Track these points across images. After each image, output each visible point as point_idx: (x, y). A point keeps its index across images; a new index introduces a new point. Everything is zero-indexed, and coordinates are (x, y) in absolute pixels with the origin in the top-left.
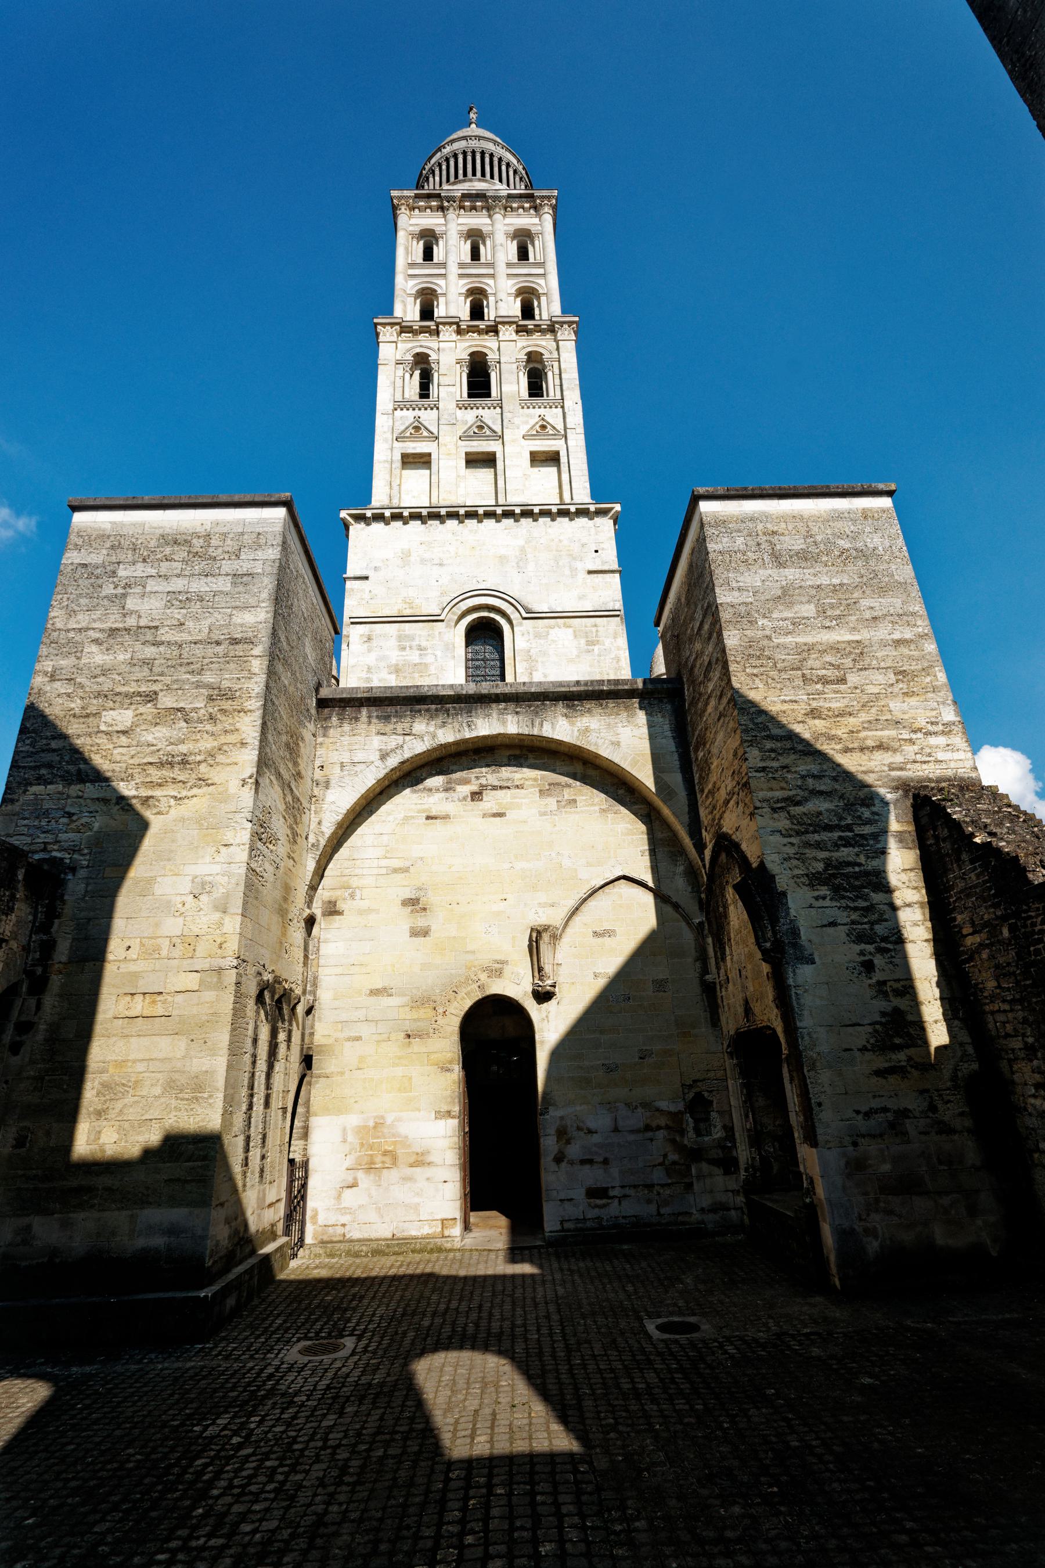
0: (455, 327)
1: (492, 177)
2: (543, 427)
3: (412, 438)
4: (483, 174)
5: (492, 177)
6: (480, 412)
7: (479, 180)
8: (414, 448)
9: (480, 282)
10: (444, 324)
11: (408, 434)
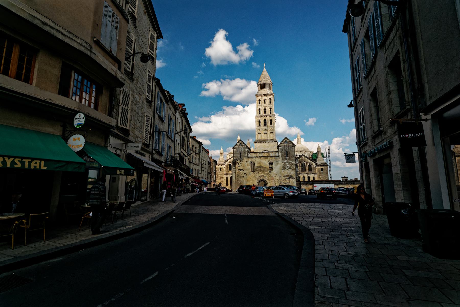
3: (259, 131)
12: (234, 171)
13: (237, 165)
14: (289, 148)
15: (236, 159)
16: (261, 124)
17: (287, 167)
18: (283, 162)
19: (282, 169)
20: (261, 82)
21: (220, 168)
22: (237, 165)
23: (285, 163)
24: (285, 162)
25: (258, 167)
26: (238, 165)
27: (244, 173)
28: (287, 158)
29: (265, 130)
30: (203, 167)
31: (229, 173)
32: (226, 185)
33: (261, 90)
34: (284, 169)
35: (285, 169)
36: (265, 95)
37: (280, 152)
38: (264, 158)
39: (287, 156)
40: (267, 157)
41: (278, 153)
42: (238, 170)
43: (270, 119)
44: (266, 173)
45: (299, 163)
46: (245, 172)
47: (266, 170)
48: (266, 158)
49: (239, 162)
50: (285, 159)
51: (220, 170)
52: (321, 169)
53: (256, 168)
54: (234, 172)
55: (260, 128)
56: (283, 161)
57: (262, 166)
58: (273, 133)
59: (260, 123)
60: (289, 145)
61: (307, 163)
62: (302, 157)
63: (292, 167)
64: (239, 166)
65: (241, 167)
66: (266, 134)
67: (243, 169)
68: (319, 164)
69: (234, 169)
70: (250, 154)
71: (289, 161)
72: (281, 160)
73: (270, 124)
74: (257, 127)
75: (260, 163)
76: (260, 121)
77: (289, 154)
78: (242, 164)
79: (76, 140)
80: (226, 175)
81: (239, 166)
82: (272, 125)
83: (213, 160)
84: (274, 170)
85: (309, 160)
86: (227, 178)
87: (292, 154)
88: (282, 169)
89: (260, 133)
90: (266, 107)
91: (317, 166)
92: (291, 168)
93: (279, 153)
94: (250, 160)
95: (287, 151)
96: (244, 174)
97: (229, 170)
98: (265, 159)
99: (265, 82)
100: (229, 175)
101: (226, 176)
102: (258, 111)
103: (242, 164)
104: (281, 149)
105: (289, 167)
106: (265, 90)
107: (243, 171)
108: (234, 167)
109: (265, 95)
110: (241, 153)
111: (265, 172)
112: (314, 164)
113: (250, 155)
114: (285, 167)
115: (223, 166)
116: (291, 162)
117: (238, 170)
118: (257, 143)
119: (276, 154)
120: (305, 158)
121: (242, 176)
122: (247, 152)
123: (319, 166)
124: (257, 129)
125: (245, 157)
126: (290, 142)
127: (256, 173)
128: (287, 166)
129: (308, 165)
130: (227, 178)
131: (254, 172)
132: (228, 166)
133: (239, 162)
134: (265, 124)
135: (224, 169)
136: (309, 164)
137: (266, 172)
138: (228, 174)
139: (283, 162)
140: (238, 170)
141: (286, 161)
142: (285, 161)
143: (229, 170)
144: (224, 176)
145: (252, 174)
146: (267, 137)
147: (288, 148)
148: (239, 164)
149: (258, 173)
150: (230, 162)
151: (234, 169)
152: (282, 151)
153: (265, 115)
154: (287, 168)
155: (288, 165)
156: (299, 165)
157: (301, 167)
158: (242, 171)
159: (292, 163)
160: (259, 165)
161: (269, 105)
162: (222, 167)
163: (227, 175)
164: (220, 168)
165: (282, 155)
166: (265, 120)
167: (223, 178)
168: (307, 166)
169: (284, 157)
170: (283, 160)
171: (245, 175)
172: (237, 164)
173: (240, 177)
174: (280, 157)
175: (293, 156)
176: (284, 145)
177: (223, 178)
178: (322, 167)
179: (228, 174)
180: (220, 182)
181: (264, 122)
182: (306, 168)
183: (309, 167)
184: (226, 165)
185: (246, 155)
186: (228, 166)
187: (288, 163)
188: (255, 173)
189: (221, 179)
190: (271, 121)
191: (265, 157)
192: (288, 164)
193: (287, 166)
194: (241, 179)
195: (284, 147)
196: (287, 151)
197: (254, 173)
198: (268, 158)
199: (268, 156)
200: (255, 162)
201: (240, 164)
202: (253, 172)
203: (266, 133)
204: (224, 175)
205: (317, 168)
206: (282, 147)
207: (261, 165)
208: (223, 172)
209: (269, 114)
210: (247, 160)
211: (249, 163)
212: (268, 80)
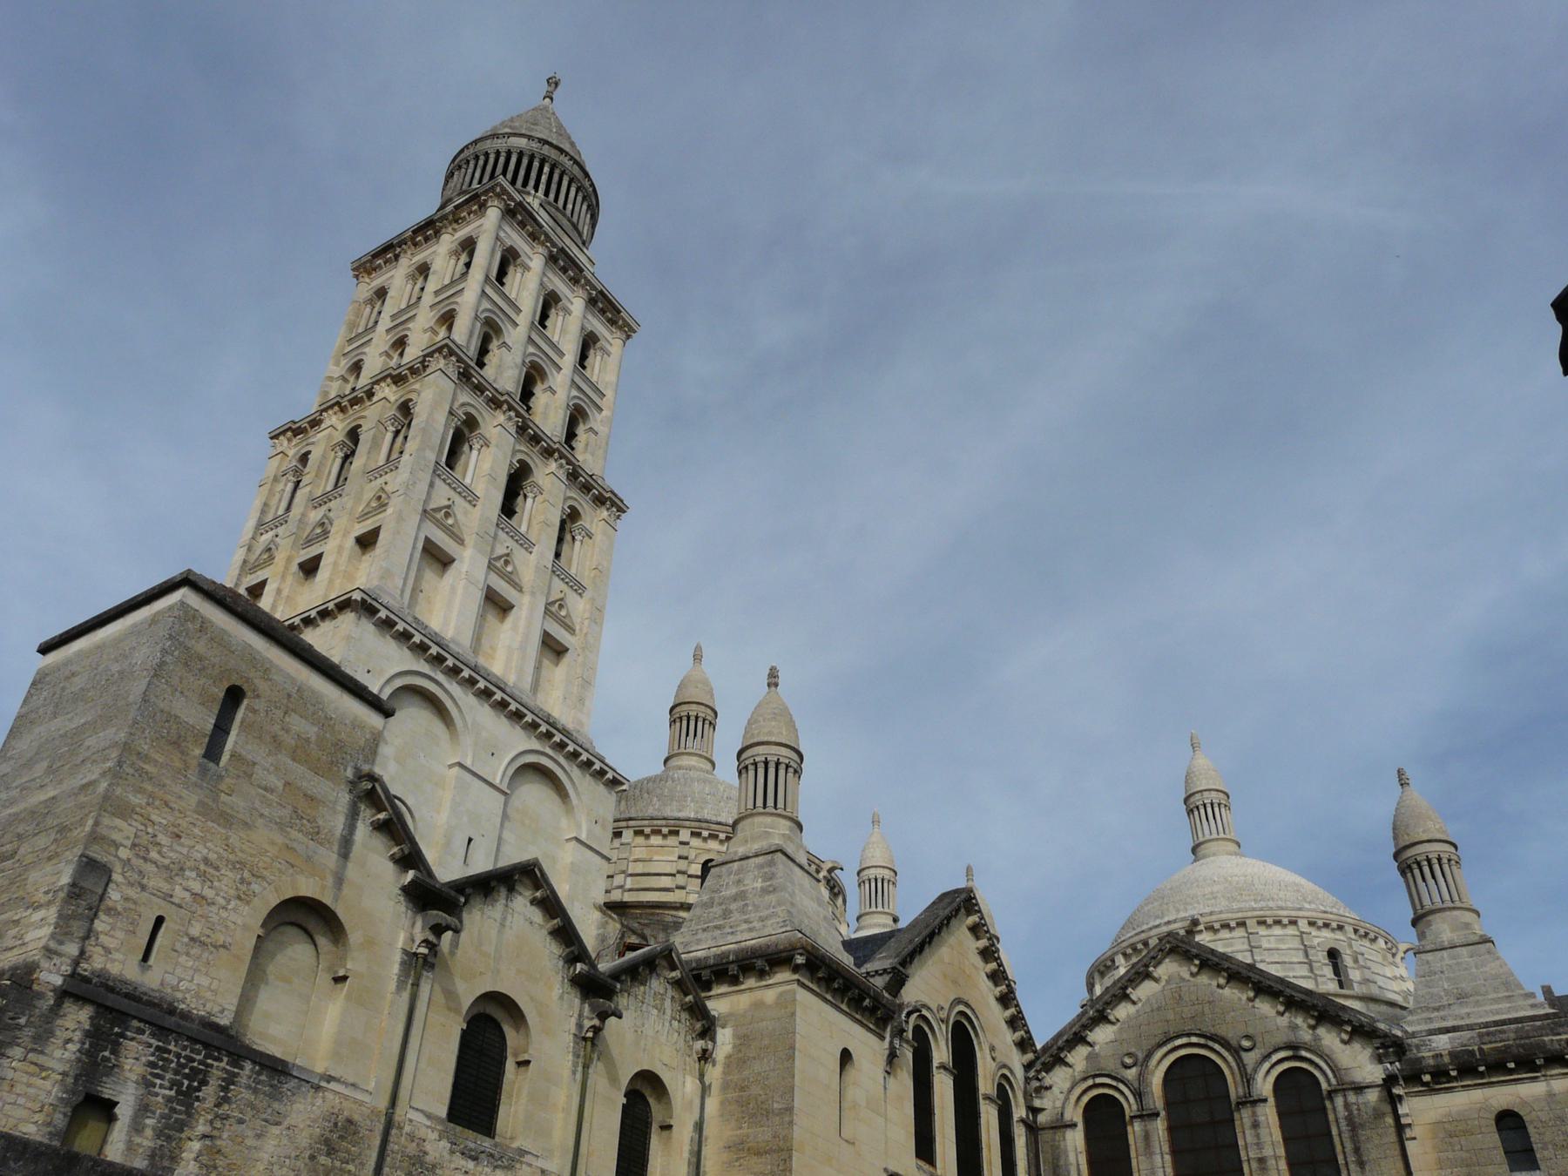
0: (336, 408)
45: (1131, 1074)
52: (1492, 1139)
61: (1249, 1058)
68: (1443, 1043)
91: (1413, 1077)
112: (1363, 1065)
123: (1439, 1077)
129: (1264, 1085)
156: (1130, 1106)
157: (1160, 1125)
168: (1251, 1101)
178: (1503, 1095)
182: (1245, 1137)
205: (1421, 1110)
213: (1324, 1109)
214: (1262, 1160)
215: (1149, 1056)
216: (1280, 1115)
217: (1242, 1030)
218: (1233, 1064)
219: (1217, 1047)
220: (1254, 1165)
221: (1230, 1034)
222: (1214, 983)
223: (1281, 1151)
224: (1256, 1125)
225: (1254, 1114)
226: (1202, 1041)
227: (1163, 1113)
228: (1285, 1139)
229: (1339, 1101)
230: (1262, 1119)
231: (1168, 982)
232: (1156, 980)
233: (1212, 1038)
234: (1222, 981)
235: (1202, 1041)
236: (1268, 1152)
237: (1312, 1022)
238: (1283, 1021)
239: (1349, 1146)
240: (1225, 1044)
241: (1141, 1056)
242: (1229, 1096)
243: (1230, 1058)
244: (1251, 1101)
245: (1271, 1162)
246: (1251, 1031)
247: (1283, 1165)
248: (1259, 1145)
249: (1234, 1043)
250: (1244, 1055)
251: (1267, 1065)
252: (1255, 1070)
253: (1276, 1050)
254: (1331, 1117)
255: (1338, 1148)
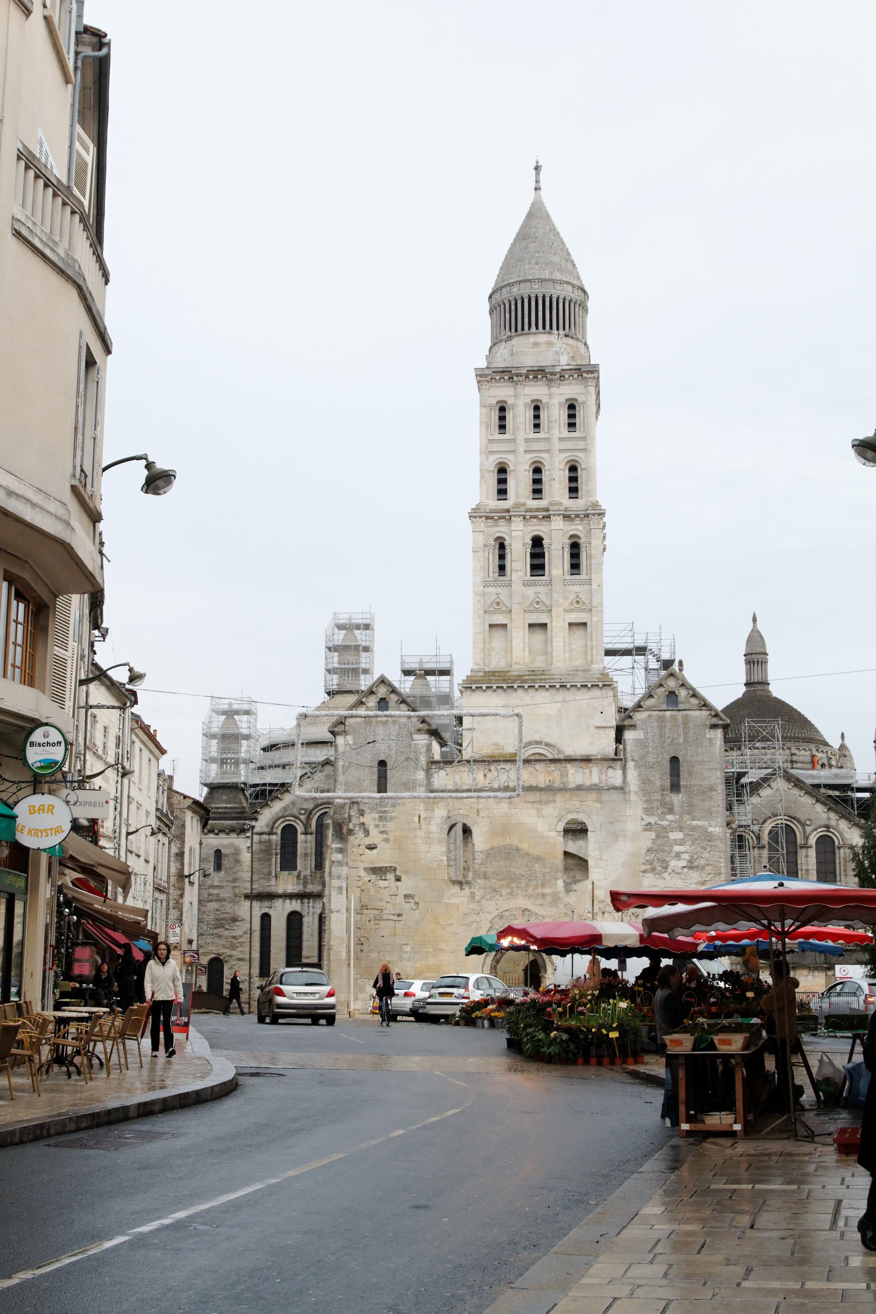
1: (551, 328)
2: (578, 602)
3: (495, 612)
4: (544, 328)
5: (551, 328)
6: (538, 589)
7: (541, 333)
8: (497, 620)
9: (539, 457)
10: (515, 516)
11: (492, 609)
12: (339, 877)
13: (357, 842)
14: (691, 734)
15: (354, 803)
16: (508, 568)
17: (678, 856)
18: (648, 827)
19: (644, 872)
20: (515, 290)
21: (218, 854)
22: (358, 839)
23: (661, 833)
24: (664, 828)
25: (491, 854)
26: (368, 841)
27: (402, 893)
28: (677, 799)
29: (537, 605)
30: (131, 852)
31: (280, 891)
32: (256, 970)
33: (515, 341)
34: (653, 870)
35: (666, 868)
36: (539, 374)
37: (630, 765)
38: (533, 796)
39: (675, 787)
40: (549, 789)
41: (618, 764)
42: (364, 868)
43: (572, 536)
44: (544, 895)
46: (407, 885)
47: (544, 874)
48: (545, 796)
49: (369, 819)
50: (663, 804)
51: (218, 867)
53: (480, 857)
54: (340, 888)
55: (503, 592)
56: (652, 820)
57: (520, 846)
58: (585, 624)
59: (502, 557)
60: (687, 716)
62: (773, 785)
63: (706, 855)
64: (371, 848)
65: (383, 857)
66: (539, 635)
67: (395, 870)
69: (340, 863)
70: (442, 773)
71: (686, 817)
72: (639, 812)
73: (567, 566)
74: (486, 584)
75: (503, 829)
76: (502, 547)
77: (690, 774)
78: (390, 835)
79: (39, 813)
80: (256, 904)
81: (371, 848)
82: (583, 576)
83: (188, 802)
84: (595, 873)
85: (819, 808)
86: (266, 919)
87: (706, 774)
88: (644, 872)
89: (504, 626)
90: (545, 456)
92: (702, 862)
93: (624, 769)
94: (440, 812)
95: (674, 760)
96: (400, 899)
97: (281, 870)
98: (540, 802)
99: (537, 290)
100: (278, 903)
101: (259, 908)
102: (493, 478)
103: (390, 835)
104: (638, 741)
105: (686, 856)
106: (543, 338)
107: (398, 879)
108: (340, 851)
109: (539, 374)
110: (382, 764)
111: (536, 887)
113: (442, 778)
114: (660, 855)
115: (242, 843)
116: (699, 823)
117: (364, 868)
118: (479, 693)
119: (610, 771)
120: (796, 792)
121: (389, 910)
122: (423, 759)
124: (484, 594)
125: (408, 786)
126: (694, 701)
127: (478, 894)
128: (677, 848)
129: (812, 841)
130: (266, 919)
131: (468, 883)
132: (274, 837)
133: (369, 819)
134: (538, 566)
135: (246, 857)
136: (821, 832)
137: (543, 885)
138: (271, 896)
139: (648, 827)
140: (362, 873)
141: (670, 817)
142: (662, 817)
143: (283, 868)
144: (244, 908)
145: (454, 901)
146: (547, 652)
147: (682, 740)
148: (373, 831)
149: (495, 891)
150: (285, 809)
151: (340, 863)
152: (642, 757)
153: (538, 510)
154: (674, 864)
155: (681, 843)
157: (765, 853)
158: (391, 876)
159: (705, 830)
160: (499, 842)
161: (561, 439)
162: (231, 845)
163: (267, 903)
164: (218, 854)
165: (645, 782)
166: (537, 542)
167: (235, 920)
168: (806, 846)
169: (657, 796)
170: (648, 811)
171: (407, 906)
172: (361, 834)
173: (378, 919)
174: (633, 797)
175: (712, 789)
176: (662, 720)
177: (235, 920)
179: (271, 896)
180: (212, 948)
181: (533, 556)
183: (817, 852)
184: (261, 834)
185: (421, 775)
186: (276, 838)
187: (681, 829)
188: (472, 895)
189: (226, 933)
190: (575, 548)
191: (541, 790)
192: (679, 835)
193: (677, 848)
194: (385, 928)
195: (661, 728)
196: (674, 760)
197: (467, 891)
198: (559, 797)
199: (557, 784)
200: (476, 823)
201: (375, 837)
202: (457, 889)
203: (544, 626)
204: (247, 903)
206: (646, 732)
207: (515, 842)
208: (235, 880)
209: (567, 502)
210: (421, 807)
211: (434, 828)
212: (558, 276)
213: (834, 853)
214: (807, 870)
215: (764, 823)
216: (817, 853)
217: (807, 816)
218: (801, 830)
219: (795, 822)
220: (804, 872)
221: (802, 818)
222: (798, 794)
223: (815, 867)
224: (807, 856)
225: (807, 852)
226: (789, 819)
227: (767, 846)
228: (817, 862)
229: (842, 851)
230: (809, 854)
231: (777, 790)
232: (772, 788)
233: (793, 818)
234: (802, 794)
235: (789, 819)
236: (810, 867)
237: (838, 818)
238: (825, 816)
239: (842, 868)
240: (799, 821)
241: (761, 821)
242: (796, 843)
243: (800, 828)
244: (806, 846)
245: (811, 871)
246: (811, 818)
247: (815, 873)
248: (807, 864)
249: (803, 821)
250: (806, 827)
251: (815, 833)
252: (810, 834)
253: (820, 827)
254: (837, 856)
255: (838, 869)
